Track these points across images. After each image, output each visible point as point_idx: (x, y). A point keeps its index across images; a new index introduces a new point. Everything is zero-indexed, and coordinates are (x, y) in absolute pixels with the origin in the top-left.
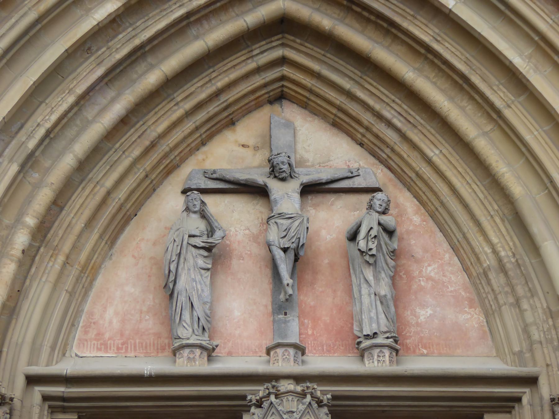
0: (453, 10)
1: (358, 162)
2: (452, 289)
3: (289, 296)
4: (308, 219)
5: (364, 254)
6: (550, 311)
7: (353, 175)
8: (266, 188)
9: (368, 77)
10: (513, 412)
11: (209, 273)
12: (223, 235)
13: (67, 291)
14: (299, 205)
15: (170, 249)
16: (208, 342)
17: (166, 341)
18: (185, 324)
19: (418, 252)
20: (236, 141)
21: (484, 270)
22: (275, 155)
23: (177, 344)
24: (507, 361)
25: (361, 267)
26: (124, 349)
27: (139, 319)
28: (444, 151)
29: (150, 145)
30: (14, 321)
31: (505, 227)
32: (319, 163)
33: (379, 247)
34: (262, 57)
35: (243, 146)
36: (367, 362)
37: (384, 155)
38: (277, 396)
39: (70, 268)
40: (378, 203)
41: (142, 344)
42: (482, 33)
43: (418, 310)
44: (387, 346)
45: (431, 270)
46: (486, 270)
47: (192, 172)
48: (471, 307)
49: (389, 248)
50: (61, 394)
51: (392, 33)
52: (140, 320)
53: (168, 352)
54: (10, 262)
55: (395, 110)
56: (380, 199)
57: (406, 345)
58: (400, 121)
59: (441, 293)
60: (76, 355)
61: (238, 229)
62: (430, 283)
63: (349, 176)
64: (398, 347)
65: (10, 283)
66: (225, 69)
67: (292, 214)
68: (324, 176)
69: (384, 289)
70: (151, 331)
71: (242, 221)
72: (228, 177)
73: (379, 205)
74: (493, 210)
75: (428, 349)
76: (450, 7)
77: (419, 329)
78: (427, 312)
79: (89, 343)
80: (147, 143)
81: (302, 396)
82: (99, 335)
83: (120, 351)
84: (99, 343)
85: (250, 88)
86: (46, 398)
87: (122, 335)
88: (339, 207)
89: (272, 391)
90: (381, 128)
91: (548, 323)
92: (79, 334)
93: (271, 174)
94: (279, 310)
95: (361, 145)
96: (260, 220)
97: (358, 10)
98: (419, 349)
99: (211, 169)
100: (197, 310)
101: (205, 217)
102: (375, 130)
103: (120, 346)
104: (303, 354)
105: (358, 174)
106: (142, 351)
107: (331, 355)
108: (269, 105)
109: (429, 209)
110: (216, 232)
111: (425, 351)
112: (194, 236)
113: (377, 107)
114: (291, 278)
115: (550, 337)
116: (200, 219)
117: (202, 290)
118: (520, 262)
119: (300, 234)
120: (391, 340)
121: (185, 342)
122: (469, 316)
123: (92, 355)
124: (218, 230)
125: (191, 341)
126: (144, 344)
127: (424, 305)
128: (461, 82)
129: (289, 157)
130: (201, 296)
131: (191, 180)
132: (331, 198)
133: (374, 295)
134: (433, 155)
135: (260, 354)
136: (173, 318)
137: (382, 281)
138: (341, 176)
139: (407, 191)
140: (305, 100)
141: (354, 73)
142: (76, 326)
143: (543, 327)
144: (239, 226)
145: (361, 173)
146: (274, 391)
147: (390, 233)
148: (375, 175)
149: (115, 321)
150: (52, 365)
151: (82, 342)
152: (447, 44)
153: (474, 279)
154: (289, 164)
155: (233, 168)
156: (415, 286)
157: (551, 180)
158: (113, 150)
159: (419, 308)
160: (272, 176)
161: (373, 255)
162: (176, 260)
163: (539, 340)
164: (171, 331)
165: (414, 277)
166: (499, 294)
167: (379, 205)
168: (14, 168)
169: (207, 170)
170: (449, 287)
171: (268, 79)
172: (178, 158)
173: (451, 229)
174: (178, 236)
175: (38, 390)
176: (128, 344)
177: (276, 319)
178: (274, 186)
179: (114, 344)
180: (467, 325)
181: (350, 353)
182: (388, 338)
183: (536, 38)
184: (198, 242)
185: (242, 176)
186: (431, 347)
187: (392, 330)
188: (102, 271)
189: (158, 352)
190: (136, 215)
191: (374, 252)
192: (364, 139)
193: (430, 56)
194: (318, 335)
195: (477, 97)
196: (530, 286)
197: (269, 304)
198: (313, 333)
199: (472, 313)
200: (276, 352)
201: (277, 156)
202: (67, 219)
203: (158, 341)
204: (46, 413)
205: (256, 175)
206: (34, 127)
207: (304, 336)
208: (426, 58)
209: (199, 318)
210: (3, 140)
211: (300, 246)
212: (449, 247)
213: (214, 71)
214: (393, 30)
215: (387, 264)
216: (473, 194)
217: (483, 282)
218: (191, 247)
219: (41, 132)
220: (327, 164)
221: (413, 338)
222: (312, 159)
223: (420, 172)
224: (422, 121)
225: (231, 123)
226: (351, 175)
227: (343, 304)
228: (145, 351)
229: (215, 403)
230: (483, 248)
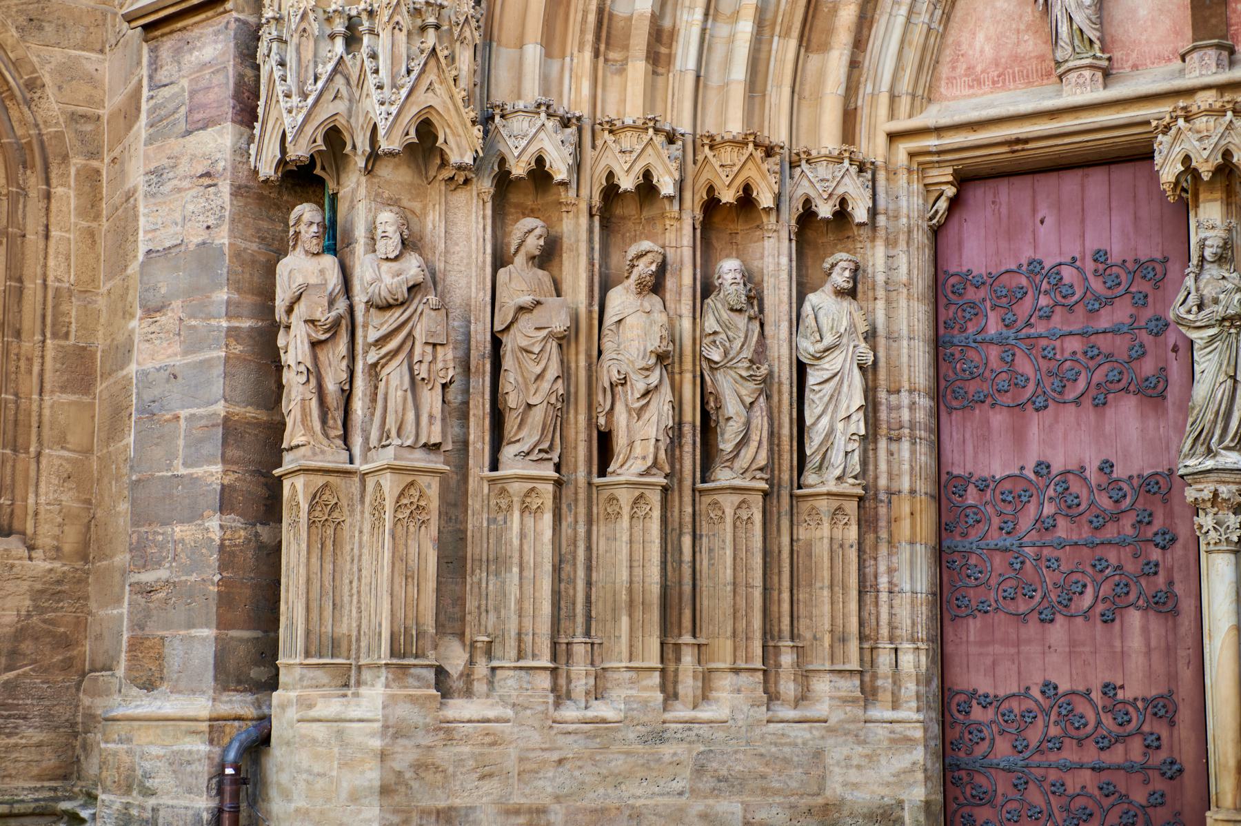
38: (1187, 119)
53: (1054, 79)
82: (970, 68)
87: (997, 65)
149: (987, 48)
175: (904, 147)
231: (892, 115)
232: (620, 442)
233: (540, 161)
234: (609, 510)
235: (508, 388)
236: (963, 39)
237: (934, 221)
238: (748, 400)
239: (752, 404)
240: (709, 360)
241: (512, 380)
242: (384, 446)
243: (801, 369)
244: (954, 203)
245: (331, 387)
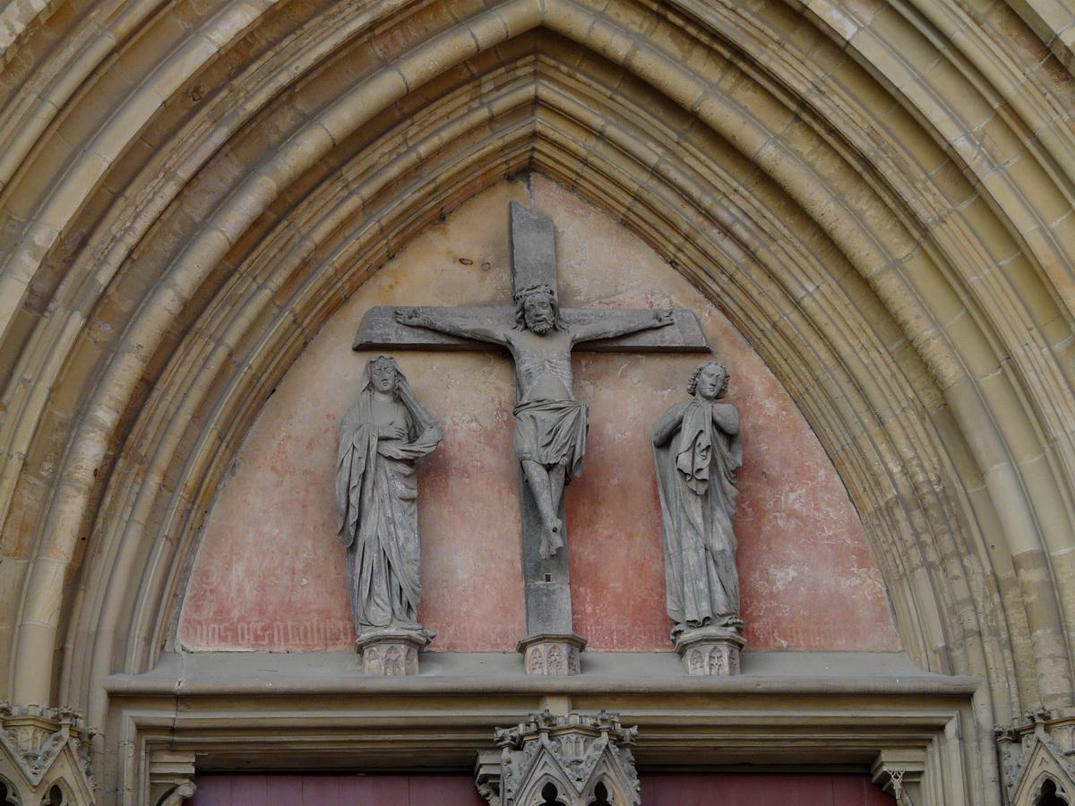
0: (853, 43)
1: (668, 297)
2: (830, 534)
3: (556, 550)
4: (587, 410)
5: (688, 478)
6: (996, 579)
7: (661, 324)
8: (509, 347)
9: (691, 143)
10: (930, 749)
11: (414, 507)
12: (438, 439)
13: (167, 537)
14: (571, 382)
15: (346, 464)
16: (420, 632)
17: (341, 625)
18: (379, 601)
19: (774, 467)
20: (449, 252)
21: (887, 503)
22: (528, 290)
23: (365, 635)
24: (921, 661)
25: (681, 500)
26: (267, 638)
27: (290, 584)
28: (824, 288)
29: (300, 265)
30: (81, 594)
31: (925, 429)
32: (600, 297)
33: (713, 466)
34: (499, 98)
35: (461, 261)
36: (691, 667)
37: (715, 287)
39: (169, 494)
40: (709, 380)
41: (298, 629)
42: (902, 90)
43: (772, 570)
44: (726, 640)
45: (794, 498)
46: (891, 504)
47: (372, 310)
48: (861, 565)
49: (728, 464)
50: (170, 723)
51: (739, 69)
52: (293, 586)
54: (75, 493)
55: (738, 207)
56: (713, 375)
57: (753, 632)
58: (747, 228)
59: (812, 540)
61: (457, 421)
62: (793, 522)
63: (655, 326)
64: (743, 640)
65: (77, 529)
66: (433, 119)
67: (560, 402)
68: (612, 327)
69: (721, 542)
70: (312, 607)
71: (464, 405)
72: (439, 324)
73: (711, 385)
74: (906, 397)
75: (790, 640)
76: (848, 37)
77: (774, 604)
78: (788, 574)
79: (205, 627)
80: (296, 261)
81: (592, 734)
82: (222, 613)
83: (261, 642)
84: (222, 627)
85: (476, 156)
86: (142, 729)
87: (262, 613)
88: (635, 381)
89: (543, 727)
90: (712, 238)
91: (992, 600)
93: (518, 322)
94: (536, 570)
95: (673, 264)
96: (497, 403)
97: (679, 22)
98: (775, 640)
99: (407, 308)
100: (399, 574)
101: (401, 400)
102: (700, 241)
103: (259, 633)
104: (582, 649)
105: (670, 322)
106: (298, 642)
107: (625, 650)
108: (506, 182)
109: (791, 389)
110: (426, 432)
111: (784, 643)
112: (387, 439)
113: (707, 201)
114: (559, 517)
115: (994, 624)
116: (394, 404)
117: (407, 540)
118: (950, 493)
119: (576, 439)
120: (732, 629)
121: (380, 632)
122: (858, 582)
124: (428, 429)
125: (392, 631)
126: (302, 628)
127: (783, 561)
128: (859, 168)
129: (552, 292)
130: (405, 549)
131: (371, 328)
132: (622, 363)
133: (704, 550)
134: (805, 296)
135: (504, 648)
136: (356, 587)
137: (718, 525)
138: (641, 327)
139: (753, 352)
140: (574, 177)
141: (666, 135)
142: (180, 596)
143: (983, 607)
144: (460, 415)
145: (675, 321)
146: (546, 727)
147: (731, 438)
148: (698, 321)
152: (836, 99)
153: (869, 515)
154: (552, 306)
155: (445, 305)
156: (769, 528)
157: (1008, 354)
158: (237, 276)
159: (775, 568)
160: (521, 327)
161: (704, 481)
162: (360, 484)
163: (976, 629)
164: (349, 605)
165: (765, 511)
166: (912, 547)
167: (711, 385)
168: (77, 321)
169: (401, 309)
170: (825, 529)
171: (508, 139)
172: (347, 286)
173: (832, 429)
174: (360, 439)
175: (130, 717)
176: (272, 627)
177: (532, 587)
178: (523, 342)
179: (248, 629)
180: (854, 597)
181: (658, 646)
182: (726, 625)
183: (996, 106)
184: (394, 449)
185: (468, 325)
186: (795, 635)
187: (733, 611)
188: (220, 495)
189: (326, 645)
190: (274, 391)
191: (705, 475)
192: (680, 255)
193: (806, 118)
194: (603, 614)
195: (887, 199)
196: (965, 534)
197: (518, 558)
198: (594, 610)
199: (864, 576)
200: (537, 650)
201: (530, 292)
202: (160, 406)
203: (325, 625)
204: (143, 754)
205: (489, 320)
206: (106, 244)
207: (579, 616)
208: (797, 118)
209: (401, 589)
210: (52, 267)
211: (575, 461)
212: (827, 458)
213: (412, 124)
214: (742, 65)
215: (724, 493)
216: (871, 368)
217: (884, 524)
218: (382, 459)
219: (120, 252)
220: (613, 299)
221: (764, 619)
222: (586, 289)
223: (781, 324)
224: (785, 231)
225: (441, 218)
226: (658, 324)
227: (645, 558)
228: (303, 642)
229: (435, 737)
230: (885, 465)
231: (117, 667)
236: (213, 568)
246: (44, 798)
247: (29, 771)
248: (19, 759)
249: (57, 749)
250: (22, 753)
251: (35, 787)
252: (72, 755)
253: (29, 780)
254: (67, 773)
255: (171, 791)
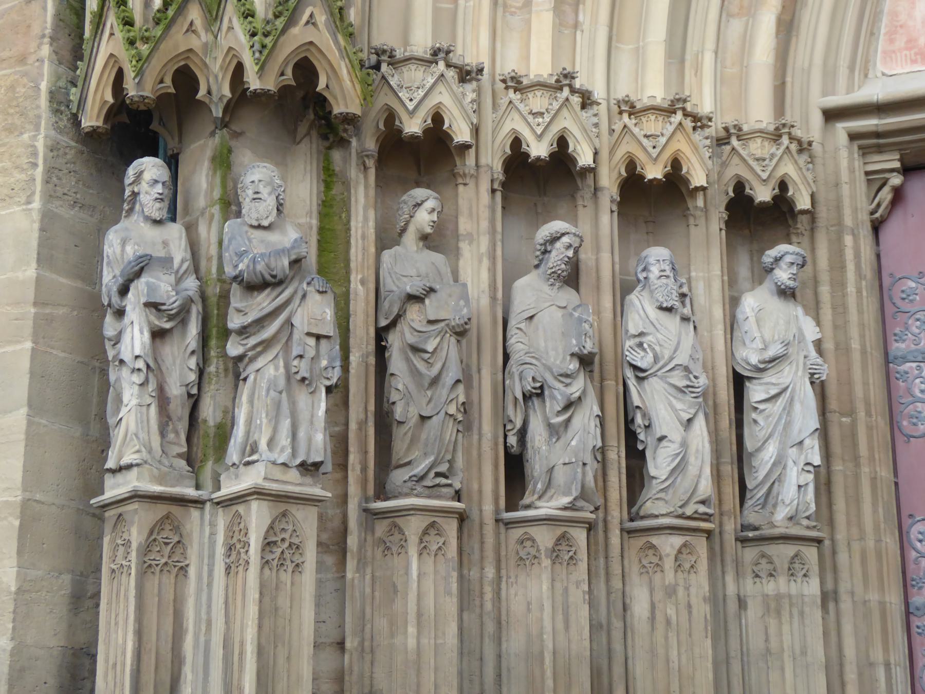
30: (794, 40)
50: (874, 129)
60: (883, 74)
79: (898, 54)
82: (911, 43)
86: (853, 137)
92: (882, 43)
123: (906, 71)
150: (853, 92)
151: (889, 55)
175: (842, 128)
204: (856, 156)
232: (536, 467)
233: (438, 118)
234: (522, 554)
235: (394, 396)
237: (877, 215)
238: (686, 416)
239: (690, 421)
240: (636, 368)
241: (400, 387)
242: (248, 464)
243: (739, 382)
244: (898, 195)
245: (175, 390)
246: (774, 189)
247: (758, 169)
248: (751, 162)
249: (780, 152)
250: (752, 157)
251: (764, 181)
252: (792, 156)
253: (759, 176)
254: (788, 169)
255: (884, 184)
